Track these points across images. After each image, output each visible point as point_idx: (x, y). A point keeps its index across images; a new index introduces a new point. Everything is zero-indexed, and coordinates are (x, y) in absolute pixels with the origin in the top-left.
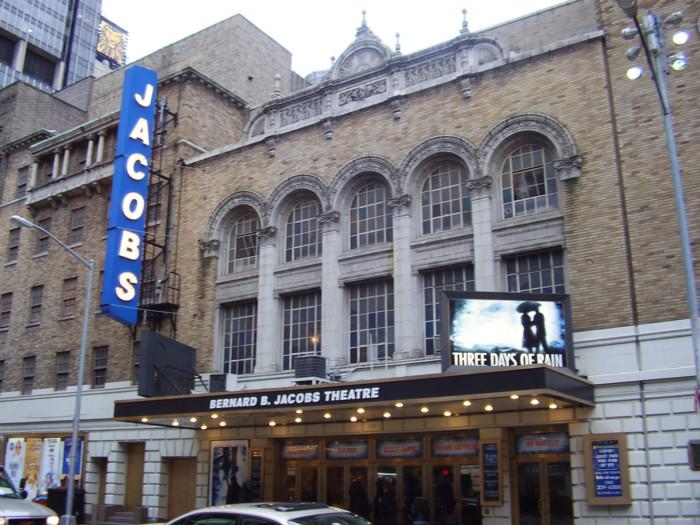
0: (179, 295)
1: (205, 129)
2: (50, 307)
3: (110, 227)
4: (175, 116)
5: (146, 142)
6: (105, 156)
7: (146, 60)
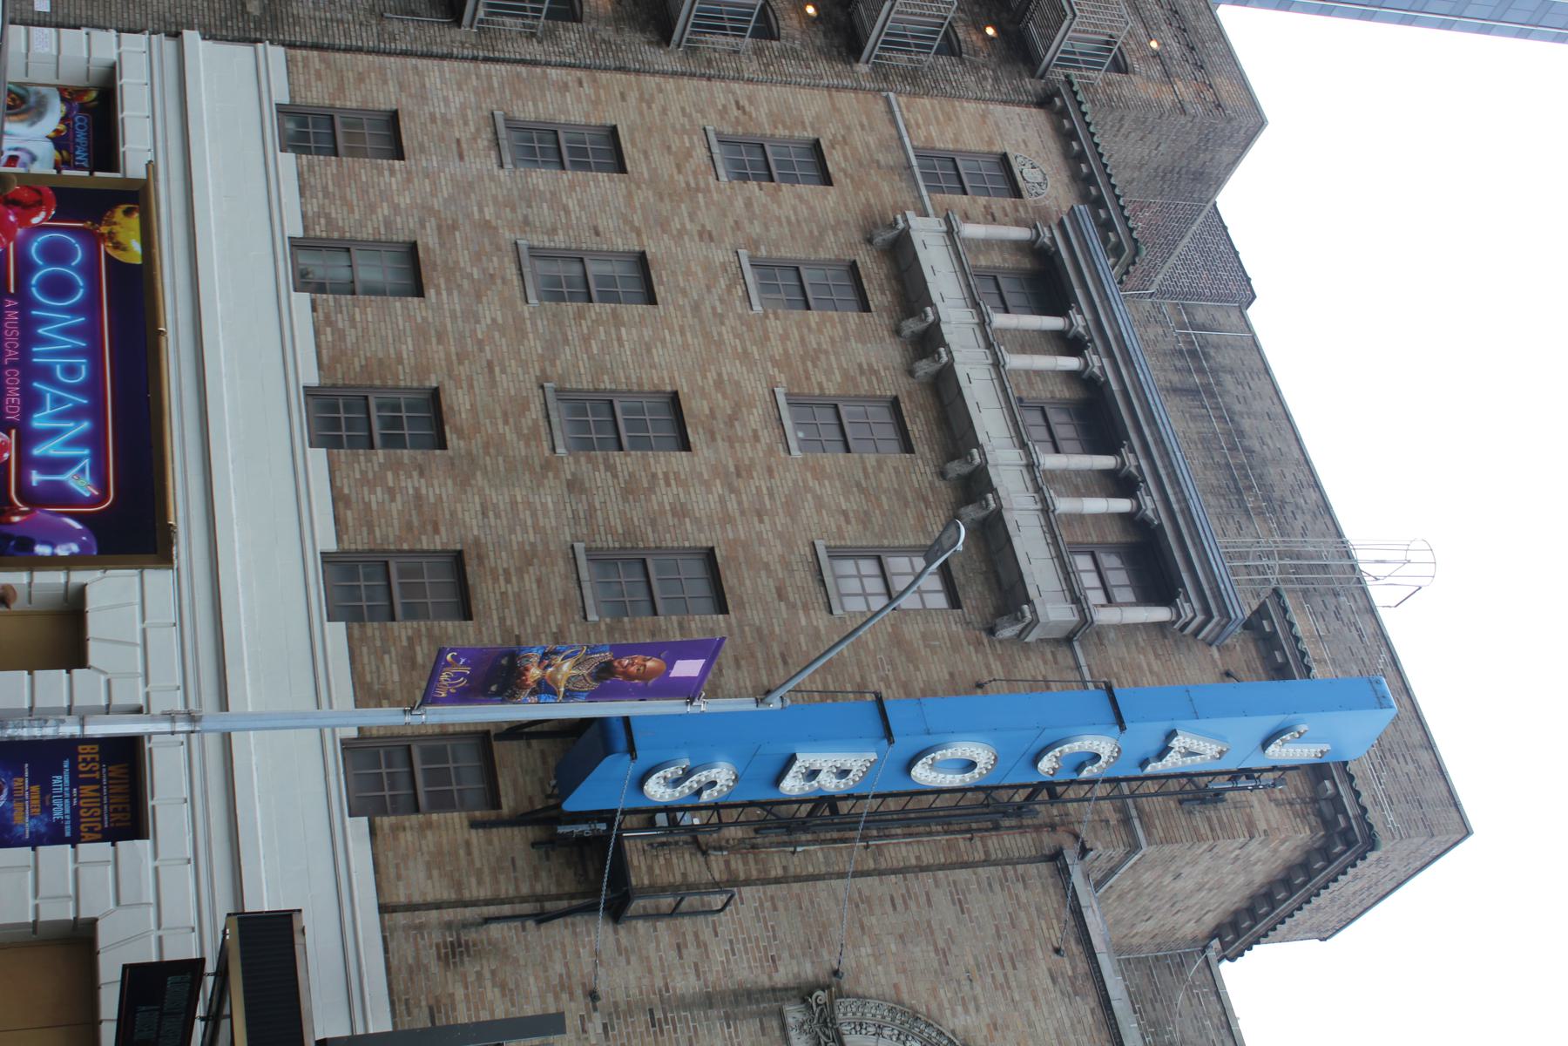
0: (658, 915)
1: (1168, 879)
2: (586, 340)
6: (1081, 518)
7: (1314, 496)
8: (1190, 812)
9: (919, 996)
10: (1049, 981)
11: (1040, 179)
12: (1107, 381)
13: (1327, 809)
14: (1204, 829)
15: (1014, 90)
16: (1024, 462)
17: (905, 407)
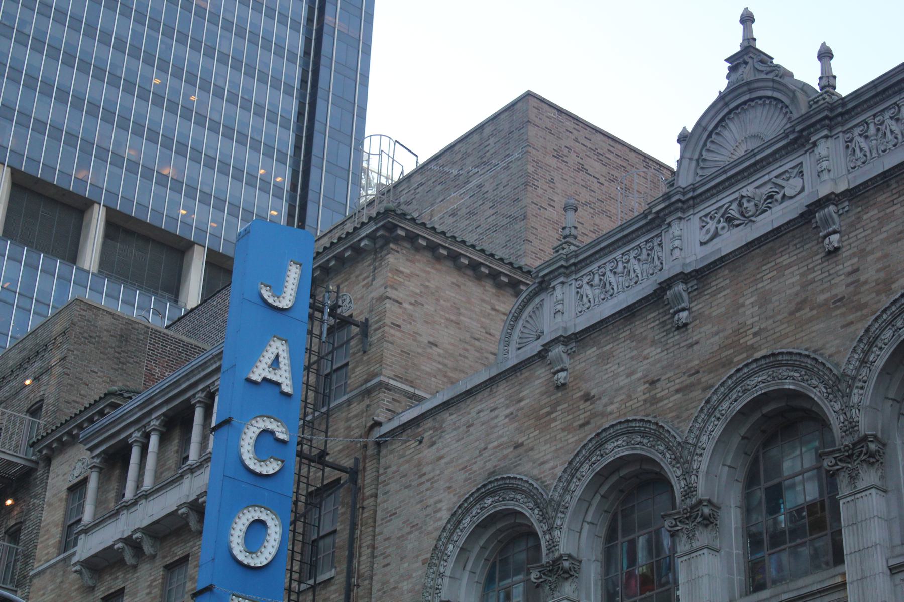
3: (200, 587)
4: (365, 326)
5: (287, 388)
8: (370, 345)
9: (429, 543)
10: (435, 447)
11: (80, 463)
12: (163, 414)
13: (380, 243)
14: (378, 334)
15: (41, 483)
16: (189, 475)
17: (169, 561)
